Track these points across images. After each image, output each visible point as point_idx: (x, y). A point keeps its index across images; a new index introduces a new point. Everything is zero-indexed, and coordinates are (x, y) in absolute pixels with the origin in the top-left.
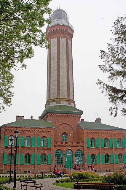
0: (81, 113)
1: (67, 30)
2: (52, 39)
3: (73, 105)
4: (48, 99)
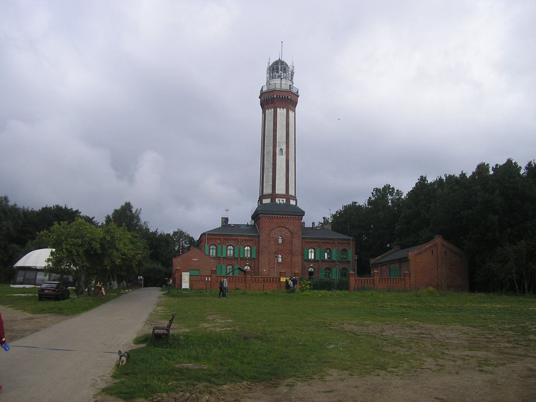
0: (302, 213)
1: (288, 97)
2: (267, 110)
3: (293, 202)
4: (261, 195)
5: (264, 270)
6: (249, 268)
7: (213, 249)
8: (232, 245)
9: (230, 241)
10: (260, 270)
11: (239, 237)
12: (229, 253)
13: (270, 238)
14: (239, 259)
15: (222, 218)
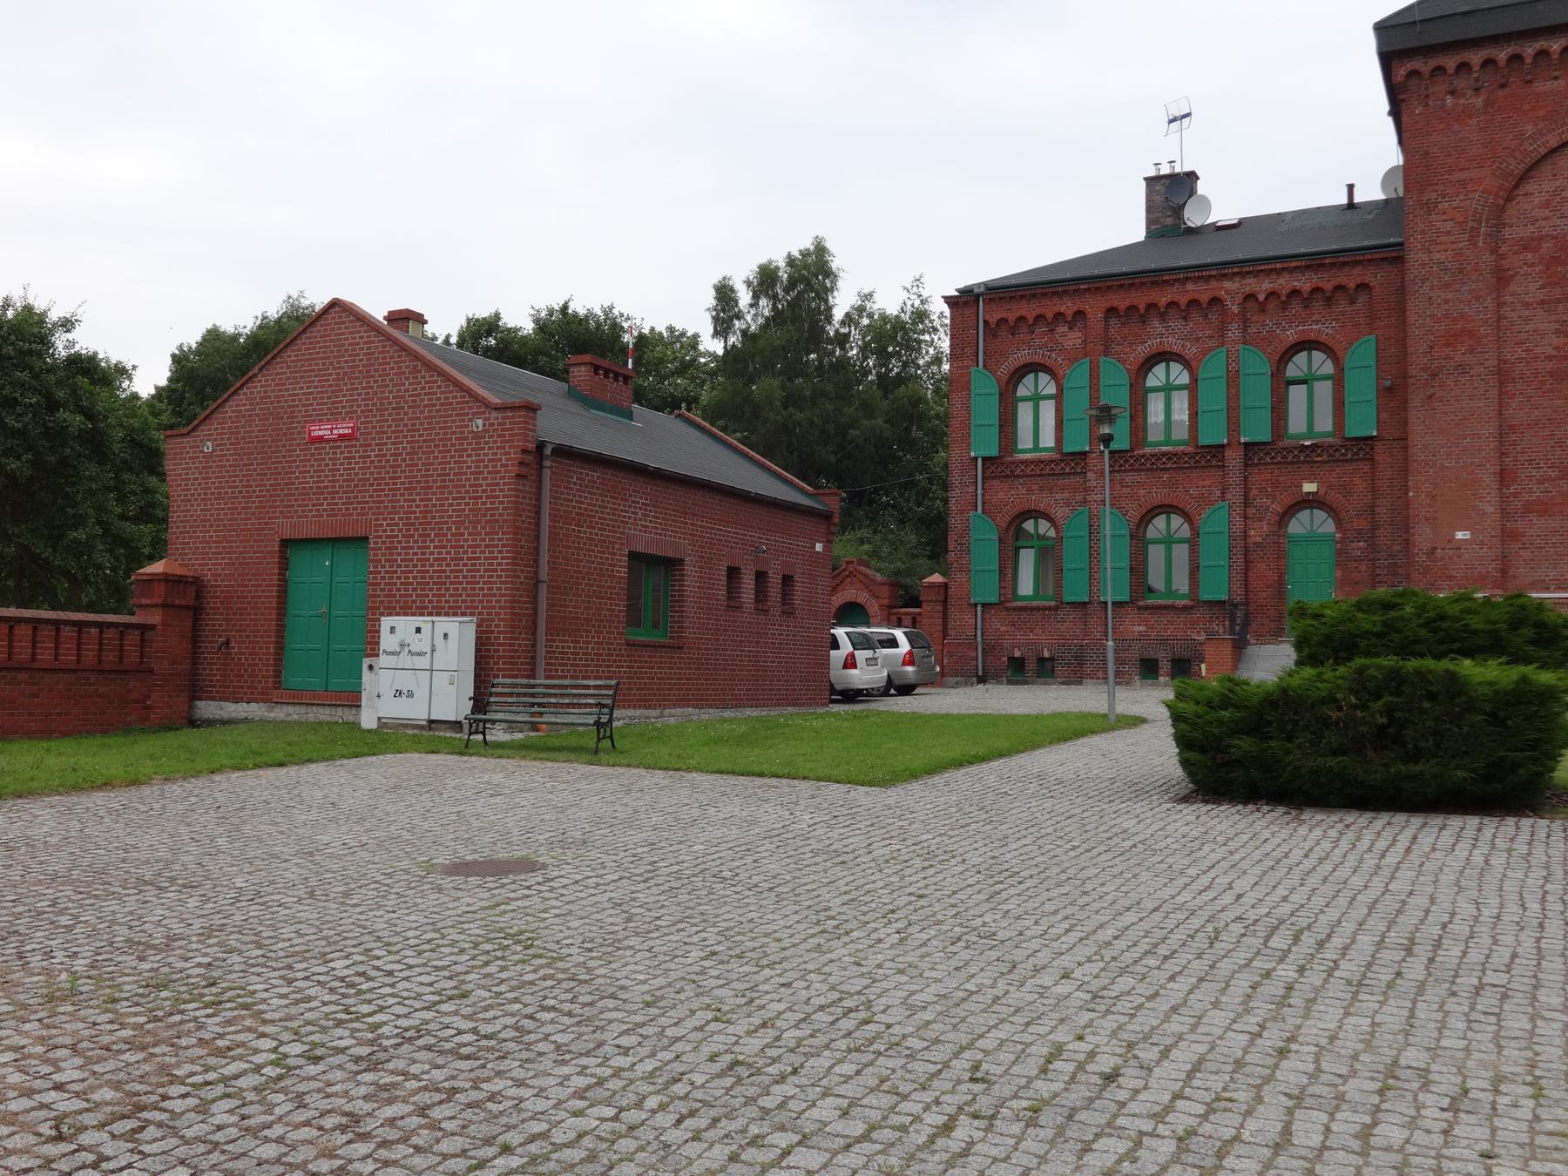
5: (1460, 535)
6: (1329, 527)
7: (1036, 399)
8: (1177, 349)
9: (1156, 324)
10: (1423, 535)
11: (1227, 284)
12: (1161, 418)
13: (1504, 249)
14: (1234, 458)
15: (1146, 179)
